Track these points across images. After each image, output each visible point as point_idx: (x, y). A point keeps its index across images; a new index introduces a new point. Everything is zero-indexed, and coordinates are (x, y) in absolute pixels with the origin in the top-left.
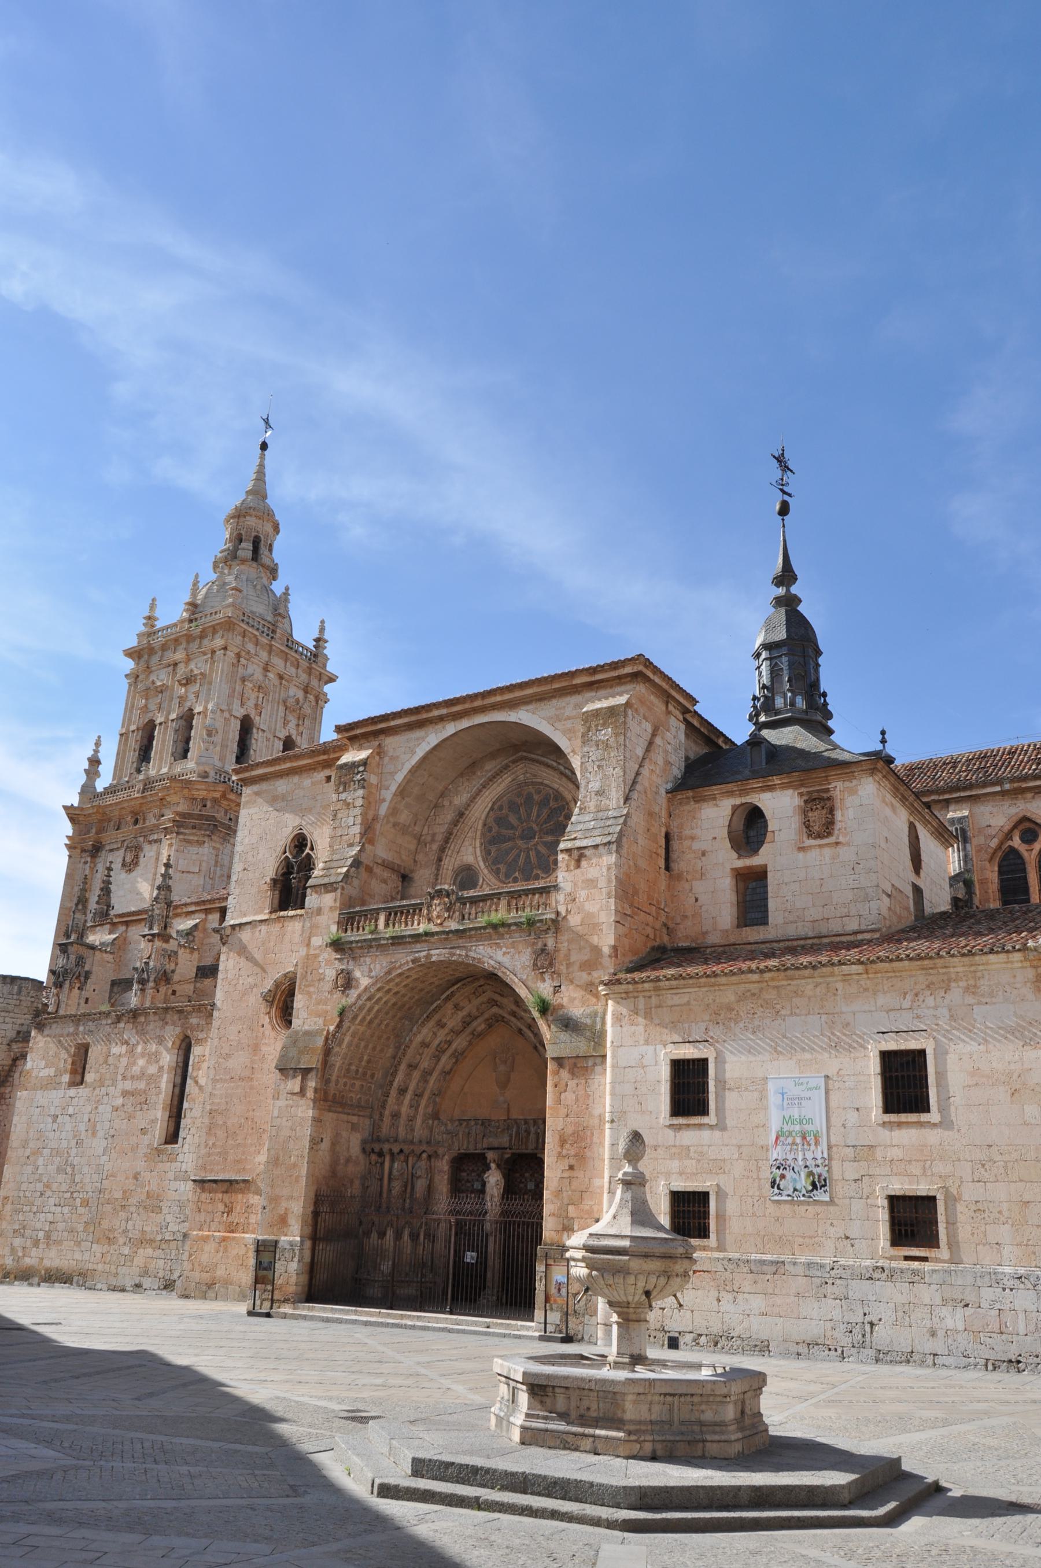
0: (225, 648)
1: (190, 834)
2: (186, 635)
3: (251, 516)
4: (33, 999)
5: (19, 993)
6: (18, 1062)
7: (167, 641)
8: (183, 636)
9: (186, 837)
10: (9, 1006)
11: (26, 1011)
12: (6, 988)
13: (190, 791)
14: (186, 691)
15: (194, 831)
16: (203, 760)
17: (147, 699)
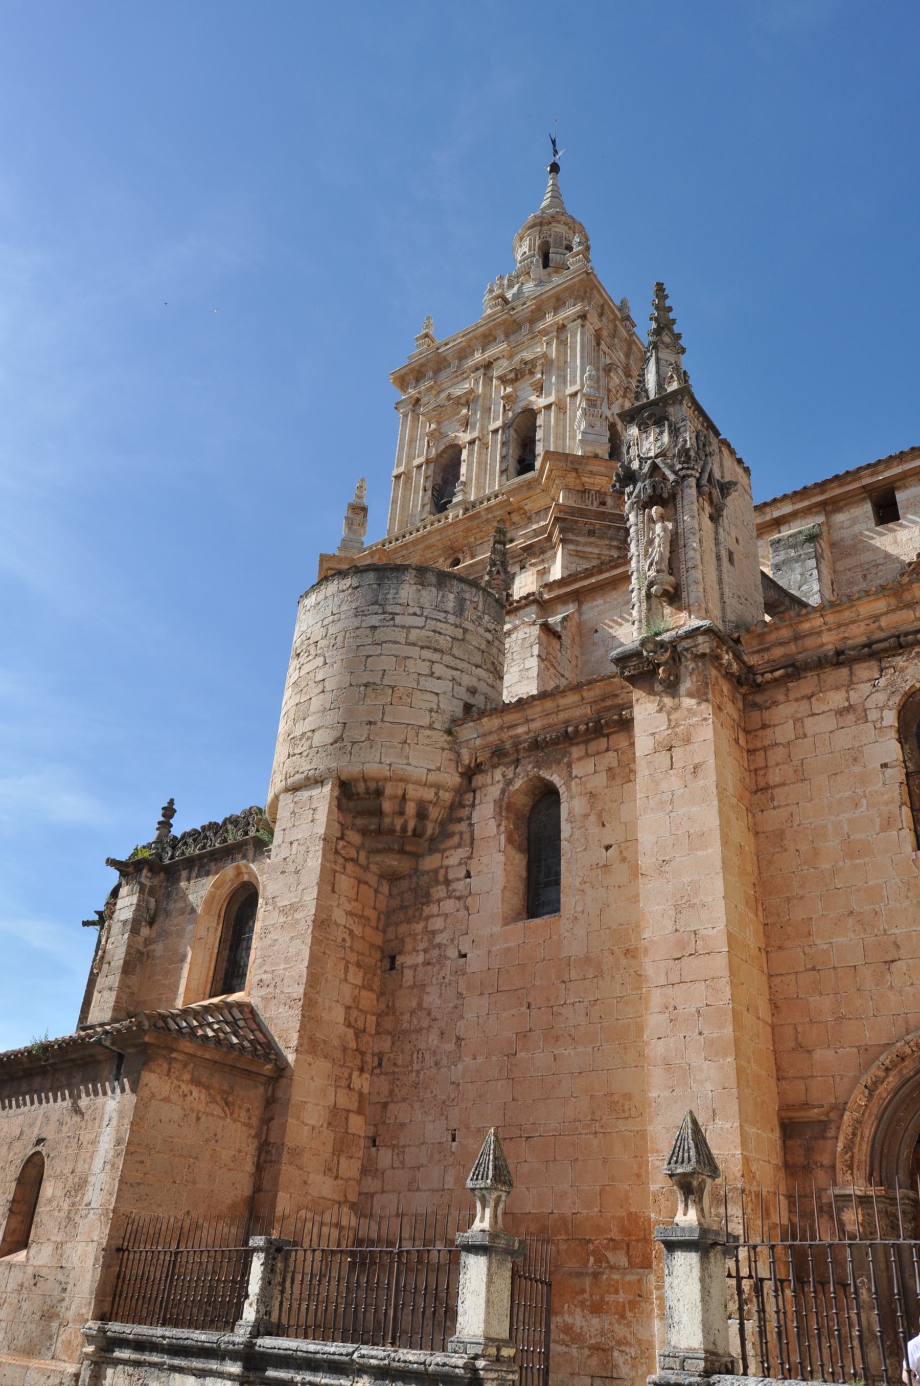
0: (583, 317)
1: (585, 544)
2: (505, 321)
3: (559, 222)
4: (489, 636)
5: (460, 610)
6: (478, 780)
7: (470, 340)
8: (499, 324)
9: (579, 548)
10: (441, 639)
11: (478, 659)
12: (429, 595)
13: (579, 477)
14: (515, 390)
15: (592, 539)
16: (591, 437)
17: (439, 423)
